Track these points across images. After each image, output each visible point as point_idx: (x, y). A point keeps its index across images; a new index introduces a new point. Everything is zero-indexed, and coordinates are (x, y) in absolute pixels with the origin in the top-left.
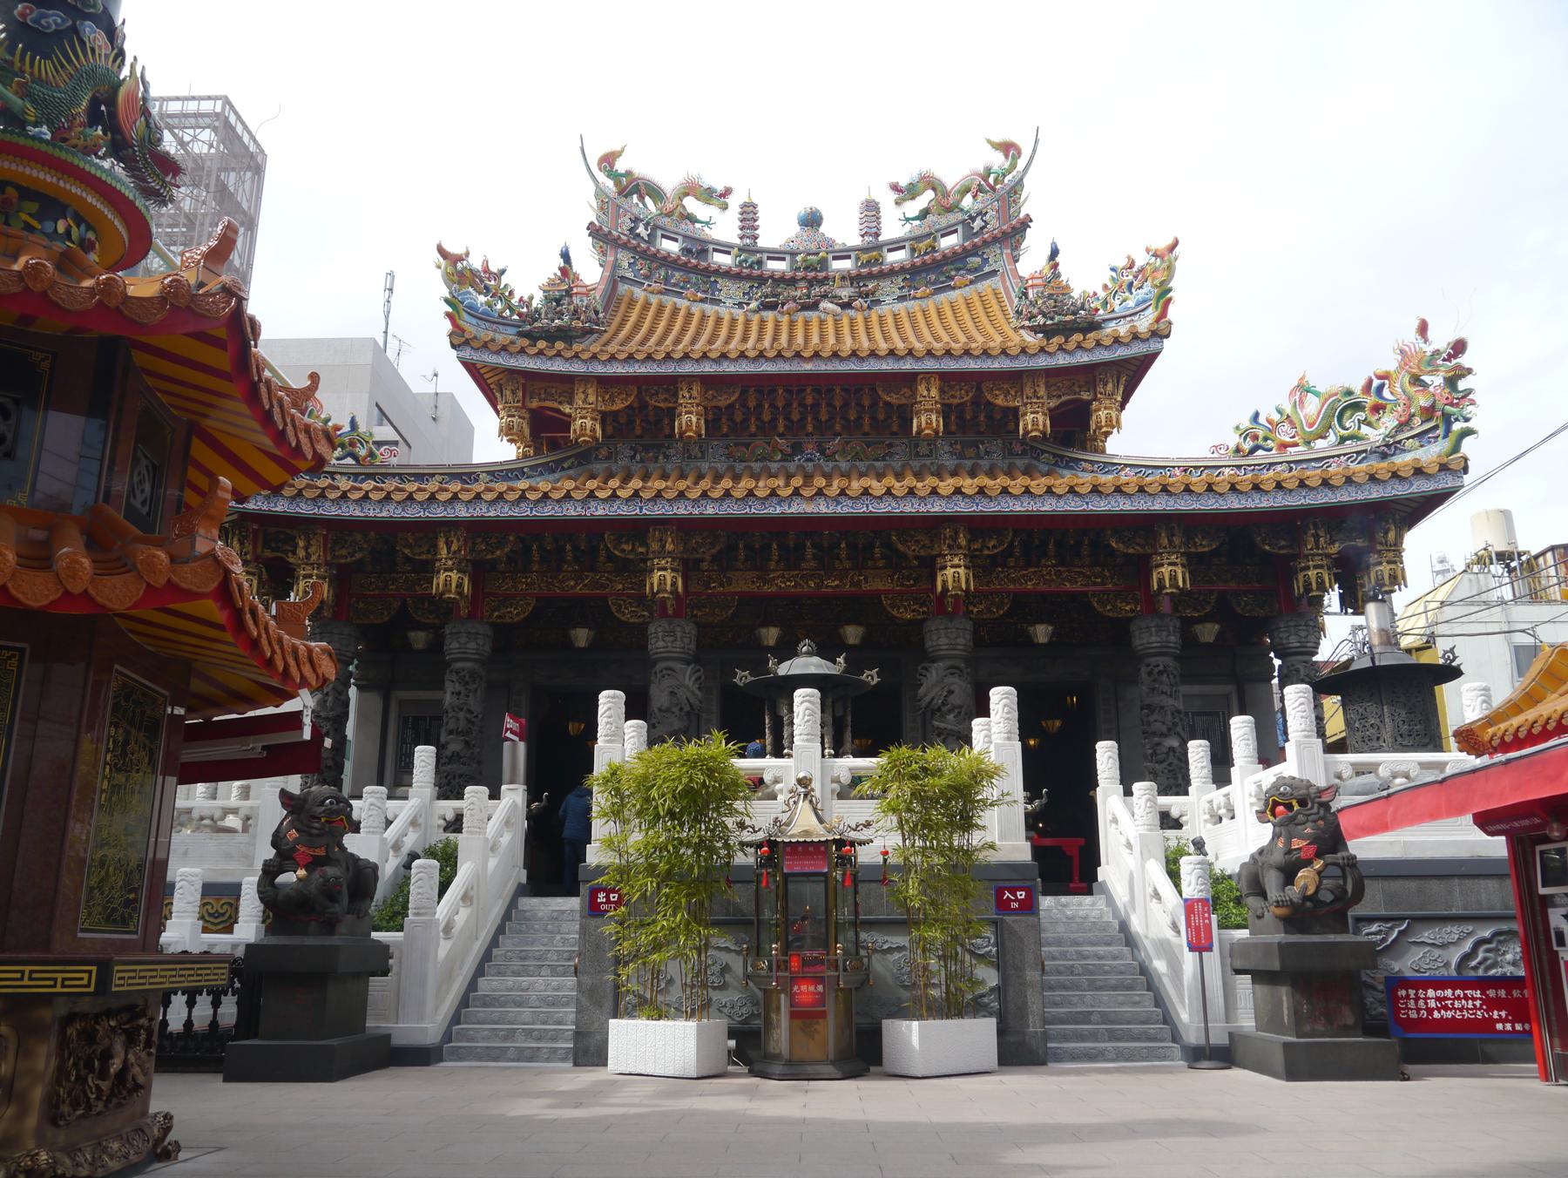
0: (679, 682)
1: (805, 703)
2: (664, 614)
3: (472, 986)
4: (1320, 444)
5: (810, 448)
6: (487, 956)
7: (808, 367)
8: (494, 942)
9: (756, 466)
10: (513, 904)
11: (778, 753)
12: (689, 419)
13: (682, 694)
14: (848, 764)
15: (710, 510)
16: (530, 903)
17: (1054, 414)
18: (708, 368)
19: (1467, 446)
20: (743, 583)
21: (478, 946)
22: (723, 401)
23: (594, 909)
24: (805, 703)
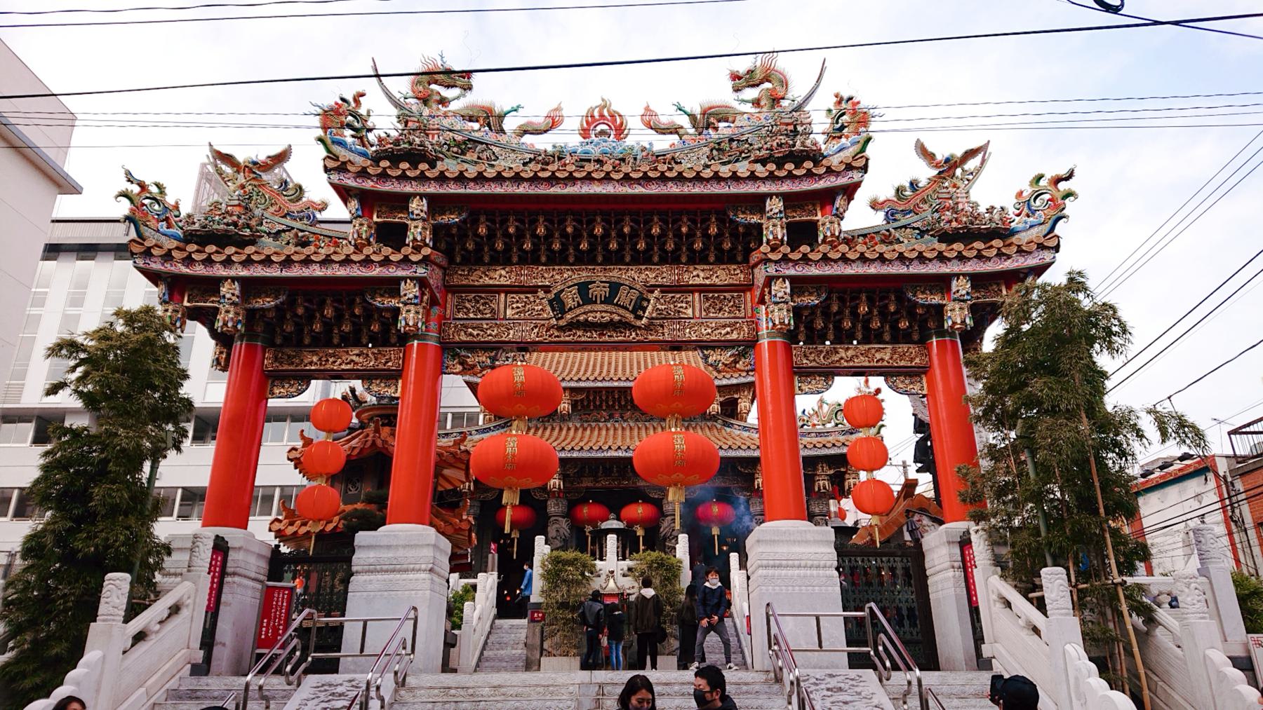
0: (561, 526)
1: (612, 540)
2: (554, 497)
3: (482, 654)
4: (829, 426)
5: (617, 416)
6: (486, 643)
7: (616, 384)
8: (488, 637)
9: (593, 424)
10: (493, 622)
11: (601, 559)
12: (565, 406)
13: (562, 531)
14: (628, 563)
15: (575, 455)
16: (497, 621)
17: (722, 404)
18: (573, 384)
19: (883, 431)
20: (587, 483)
21: (483, 638)
22: (579, 397)
23: (533, 620)
24: (612, 540)
